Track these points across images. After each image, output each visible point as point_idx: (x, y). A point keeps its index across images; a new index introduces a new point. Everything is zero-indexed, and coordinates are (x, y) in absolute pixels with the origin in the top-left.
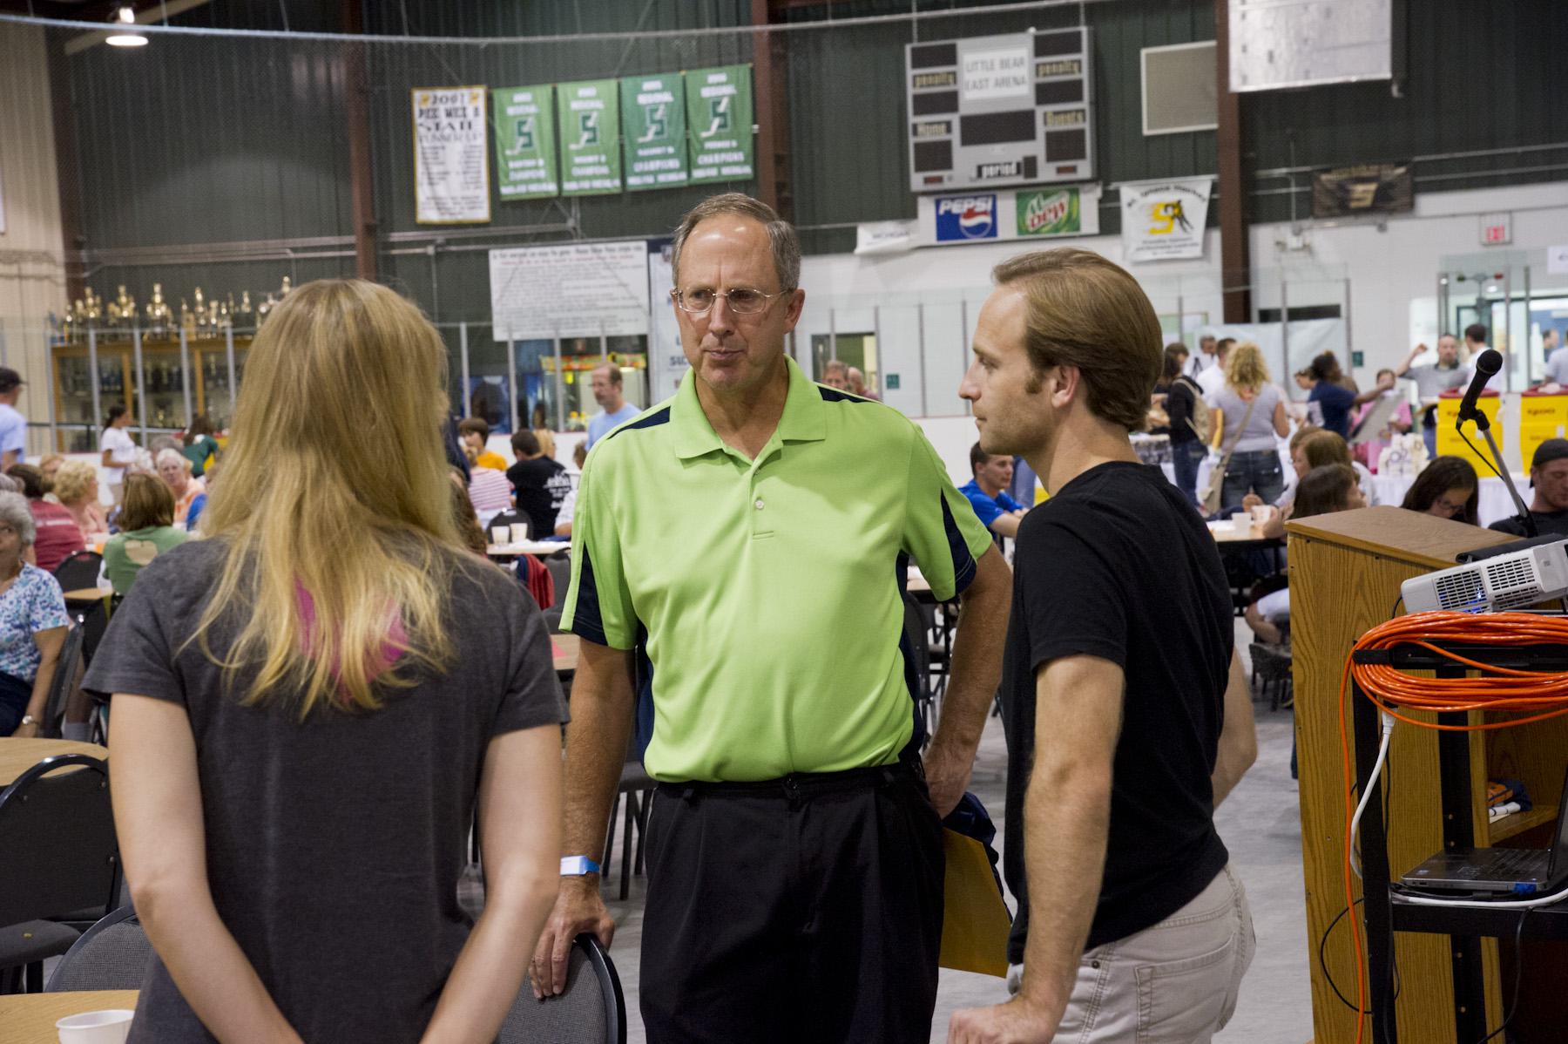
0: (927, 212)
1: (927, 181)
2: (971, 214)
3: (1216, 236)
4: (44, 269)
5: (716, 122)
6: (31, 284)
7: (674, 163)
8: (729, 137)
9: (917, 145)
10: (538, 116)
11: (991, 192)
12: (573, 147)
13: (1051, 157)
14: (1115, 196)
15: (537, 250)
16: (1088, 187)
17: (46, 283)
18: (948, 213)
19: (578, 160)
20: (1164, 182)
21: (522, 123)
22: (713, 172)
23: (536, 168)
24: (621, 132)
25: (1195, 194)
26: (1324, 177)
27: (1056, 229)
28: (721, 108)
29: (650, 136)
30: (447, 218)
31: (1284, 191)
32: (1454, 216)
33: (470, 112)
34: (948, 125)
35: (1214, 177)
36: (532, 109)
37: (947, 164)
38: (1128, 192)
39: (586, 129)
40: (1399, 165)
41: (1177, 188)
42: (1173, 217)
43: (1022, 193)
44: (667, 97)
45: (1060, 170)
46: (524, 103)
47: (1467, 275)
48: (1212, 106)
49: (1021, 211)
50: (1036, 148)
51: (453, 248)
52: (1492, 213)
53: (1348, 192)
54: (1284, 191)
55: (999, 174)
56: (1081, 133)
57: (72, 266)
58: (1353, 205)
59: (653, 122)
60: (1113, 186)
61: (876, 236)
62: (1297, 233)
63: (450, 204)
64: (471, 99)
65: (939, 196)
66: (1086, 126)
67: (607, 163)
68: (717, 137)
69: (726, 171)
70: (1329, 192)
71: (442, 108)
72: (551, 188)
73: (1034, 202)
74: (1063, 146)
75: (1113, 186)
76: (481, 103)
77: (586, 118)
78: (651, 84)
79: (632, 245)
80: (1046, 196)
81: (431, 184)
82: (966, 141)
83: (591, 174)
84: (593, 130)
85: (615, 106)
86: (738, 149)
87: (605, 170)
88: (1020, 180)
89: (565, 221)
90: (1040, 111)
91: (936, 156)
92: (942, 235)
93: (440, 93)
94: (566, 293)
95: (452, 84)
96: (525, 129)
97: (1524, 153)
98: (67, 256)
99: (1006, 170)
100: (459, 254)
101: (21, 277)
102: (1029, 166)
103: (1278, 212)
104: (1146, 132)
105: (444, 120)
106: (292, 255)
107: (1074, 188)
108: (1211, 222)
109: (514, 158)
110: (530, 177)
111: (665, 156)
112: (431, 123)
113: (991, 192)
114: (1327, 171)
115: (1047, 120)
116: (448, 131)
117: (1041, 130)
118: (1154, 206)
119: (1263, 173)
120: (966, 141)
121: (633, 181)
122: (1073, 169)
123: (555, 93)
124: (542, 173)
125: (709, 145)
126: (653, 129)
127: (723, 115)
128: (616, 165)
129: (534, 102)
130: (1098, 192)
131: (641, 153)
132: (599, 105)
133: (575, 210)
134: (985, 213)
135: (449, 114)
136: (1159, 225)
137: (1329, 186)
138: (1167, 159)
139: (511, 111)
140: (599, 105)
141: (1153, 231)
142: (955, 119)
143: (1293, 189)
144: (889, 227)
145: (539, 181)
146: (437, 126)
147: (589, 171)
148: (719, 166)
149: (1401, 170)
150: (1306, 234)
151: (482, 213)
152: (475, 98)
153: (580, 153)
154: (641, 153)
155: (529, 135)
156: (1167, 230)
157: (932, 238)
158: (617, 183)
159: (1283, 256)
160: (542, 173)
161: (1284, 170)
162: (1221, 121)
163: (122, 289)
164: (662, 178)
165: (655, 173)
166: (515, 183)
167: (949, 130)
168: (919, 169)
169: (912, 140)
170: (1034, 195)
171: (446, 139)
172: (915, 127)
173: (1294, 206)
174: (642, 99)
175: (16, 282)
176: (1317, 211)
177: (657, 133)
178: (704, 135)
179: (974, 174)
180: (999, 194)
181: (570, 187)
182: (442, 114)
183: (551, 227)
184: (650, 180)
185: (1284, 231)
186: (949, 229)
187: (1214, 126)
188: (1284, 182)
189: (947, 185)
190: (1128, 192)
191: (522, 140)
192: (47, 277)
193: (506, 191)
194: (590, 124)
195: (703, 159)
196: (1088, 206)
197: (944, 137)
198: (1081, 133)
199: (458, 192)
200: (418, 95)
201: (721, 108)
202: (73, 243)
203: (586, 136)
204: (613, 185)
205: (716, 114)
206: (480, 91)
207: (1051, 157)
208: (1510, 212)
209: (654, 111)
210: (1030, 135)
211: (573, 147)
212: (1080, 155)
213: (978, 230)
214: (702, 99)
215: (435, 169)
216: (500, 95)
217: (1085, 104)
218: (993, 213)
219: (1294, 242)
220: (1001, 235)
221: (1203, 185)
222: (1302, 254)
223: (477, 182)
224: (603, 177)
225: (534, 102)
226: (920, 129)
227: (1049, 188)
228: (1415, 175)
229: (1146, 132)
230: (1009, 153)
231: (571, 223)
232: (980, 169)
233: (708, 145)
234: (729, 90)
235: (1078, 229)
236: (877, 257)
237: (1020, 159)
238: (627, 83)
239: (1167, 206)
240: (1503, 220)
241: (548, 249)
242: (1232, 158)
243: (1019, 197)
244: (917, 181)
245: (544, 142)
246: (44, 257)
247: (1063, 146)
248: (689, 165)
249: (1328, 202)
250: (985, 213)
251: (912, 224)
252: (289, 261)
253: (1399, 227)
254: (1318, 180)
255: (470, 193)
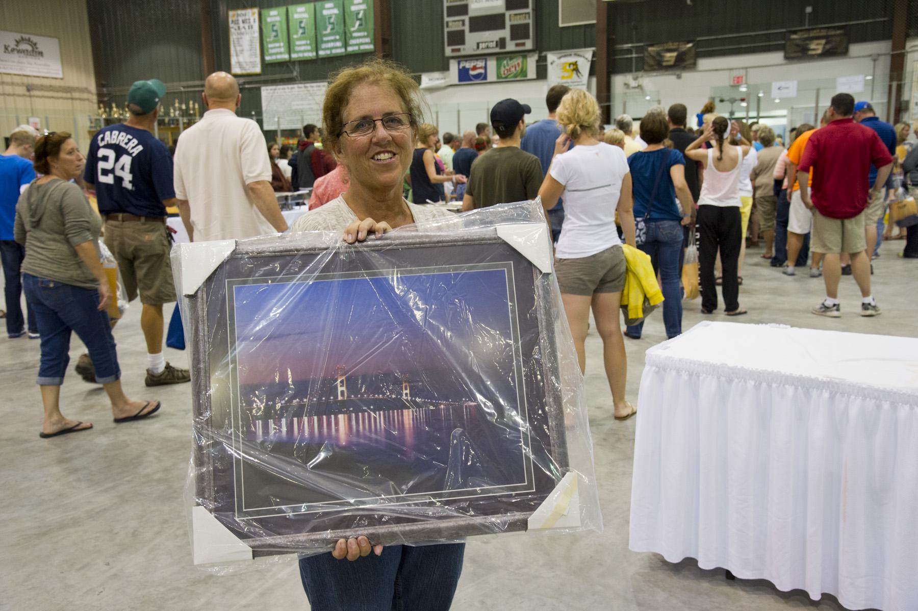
0: (454, 67)
1: (453, 51)
2: (475, 68)
3: (594, 80)
4: (85, 96)
5: (358, 23)
6: (78, 102)
7: (339, 44)
8: (363, 30)
9: (449, 33)
10: (280, 22)
11: (484, 56)
12: (295, 37)
13: (512, 38)
14: (545, 57)
15: (281, 87)
16: (531, 54)
17: (87, 102)
18: (464, 67)
19: (298, 43)
20: (568, 52)
21: (274, 26)
22: (356, 48)
23: (280, 47)
24: (316, 29)
25: (584, 58)
26: (650, 49)
27: (515, 76)
28: (360, 16)
29: (329, 31)
30: (244, 72)
31: (629, 56)
32: (716, 70)
33: (252, 21)
34: (463, 21)
35: (594, 49)
36: (278, 19)
37: (462, 42)
38: (551, 57)
39: (301, 27)
40: (689, 42)
41: (576, 55)
42: (574, 70)
43: (499, 57)
44: (336, 11)
45: (517, 45)
46: (274, 15)
47: (726, 98)
48: (594, 11)
49: (498, 67)
50: (506, 33)
51: (247, 86)
52: (736, 69)
53: (662, 57)
54: (629, 56)
55: (488, 47)
56: (528, 24)
57: (100, 95)
58: (665, 64)
59: (330, 23)
60: (543, 54)
61: (431, 80)
62: (635, 79)
63: (244, 65)
64: (252, 14)
65: (460, 59)
66: (530, 21)
67: (310, 44)
68: (358, 31)
69: (362, 47)
70: (653, 57)
71: (240, 19)
72: (286, 57)
73: (505, 62)
74: (519, 32)
75: (543, 54)
76: (256, 17)
77: (301, 22)
78: (328, 5)
79: (321, 84)
80: (511, 59)
81: (237, 55)
82: (472, 30)
83: (303, 50)
84: (304, 28)
85: (313, 16)
86: (367, 36)
87: (309, 48)
88: (497, 50)
89: (292, 72)
90: (508, 14)
91: (457, 38)
92: (460, 79)
93: (240, 12)
94: (294, 108)
95: (245, 7)
96: (275, 28)
97: (756, 35)
98: (98, 90)
99: (491, 45)
100: (249, 89)
101: (72, 99)
102: (502, 43)
103: (626, 68)
104: (561, 25)
105: (241, 25)
106: (182, 89)
107: (524, 54)
108: (592, 73)
109: (271, 43)
110: (278, 52)
111: (335, 41)
112: (236, 27)
113: (484, 56)
114: (652, 45)
115: (513, 18)
116: (243, 30)
117: (508, 24)
118: (564, 64)
119: (619, 47)
120: (472, 30)
121: (321, 53)
122: (523, 44)
123: (287, 11)
124: (282, 50)
125: (355, 35)
126: (330, 27)
127: (361, 19)
128: (314, 45)
129: (279, 15)
130: (536, 57)
131: (325, 39)
132: (306, 16)
133: (297, 67)
134: (481, 68)
135: (243, 22)
136: (566, 74)
137: (652, 53)
138: (570, 40)
139: (269, 20)
140: (306, 16)
141: (563, 77)
142: (466, 18)
143: (634, 55)
144: (436, 75)
145: (281, 53)
146: (239, 28)
147: (303, 48)
148: (359, 45)
149: (690, 45)
150: (640, 79)
151: (258, 69)
152: (253, 14)
153: (299, 39)
154: (325, 39)
155: (276, 31)
156: (570, 77)
157: (456, 81)
158: (314, 54)
159: (628, 91)
160: (282, 50)
161: (630, 45)
162: (598, 20)
163: (114, 105)
164: (334, 51)
165: (331, 49)
166: (271, 55)
167: (463, 24)
168: (449, 45)
169: (446, 30)
170: (505, 58)
171: (242, 34)
172: (447, 23)
173: (634, 64)
174: (325, 12)
175: (70, 101)
176: (646, 67)
177: (332, 29)
178: (353, 29)
179: (475, 47)
180: (488, 58)
181: (294, 56)
182: (240, 22)
183: (287, 76)
184: (328, 52)
185: (629, 78)
186: (464, 76)
187: (594, 22)
188: (629, 51)
189: (462, 53)
190: (551, 57)
191: (274, 34)
192: (88, 99)
193: (267, 58)
194: (303, 25)
195: (352, 42)
196: (531, 64)
197: (461, 28)
198: (528, 24)
199: (248, 60)
200: (231, 13)
201: (360, 16)
202: (100, 85)
203: (301, 31)
204: (312, 55)
205: (358, 19)
206: (256, 10)
207: (512, 38)
208: (746, 68)
209: (330, 18)
210: (503, 27)
211: (295, 37)
212: (527, 37)
213: (477, 77)
214: (351, 12)
215: (238, 48)
216: (264, 12)
217: (530, 10)
218: (485, 68)
219: (633, 84)
220: (490, 79)
221: (588, 53)
222: (637, 90)
223: (255, 55)
224: (308, 51)
225: (279, 15)
226: (450, 24)
227: (511, 55)
228: (698, 47)
229: (561, 25)
230: (493, 36)
231: (295, 74)
232: (478, 44)
233: (355, 35)
234: (364, 7)
235: (526, 76)
236: (431, 90)
237: (497, 39)
238: (318, 4)
239: (570, 64)
240: (742, 73)
241: (285, 87)
242: (603, 39)
243: (498, 59)
244: (448, 51)
245: (283, 35)
246: (86, 90)
247: (519, 32)
248: (346, 45)
249: (651, 62)
250: (481, 68)
251: (447, 73)
252: (181, 92)
253: (687, 75)
254: (647, 50)
255: (253, 59)
